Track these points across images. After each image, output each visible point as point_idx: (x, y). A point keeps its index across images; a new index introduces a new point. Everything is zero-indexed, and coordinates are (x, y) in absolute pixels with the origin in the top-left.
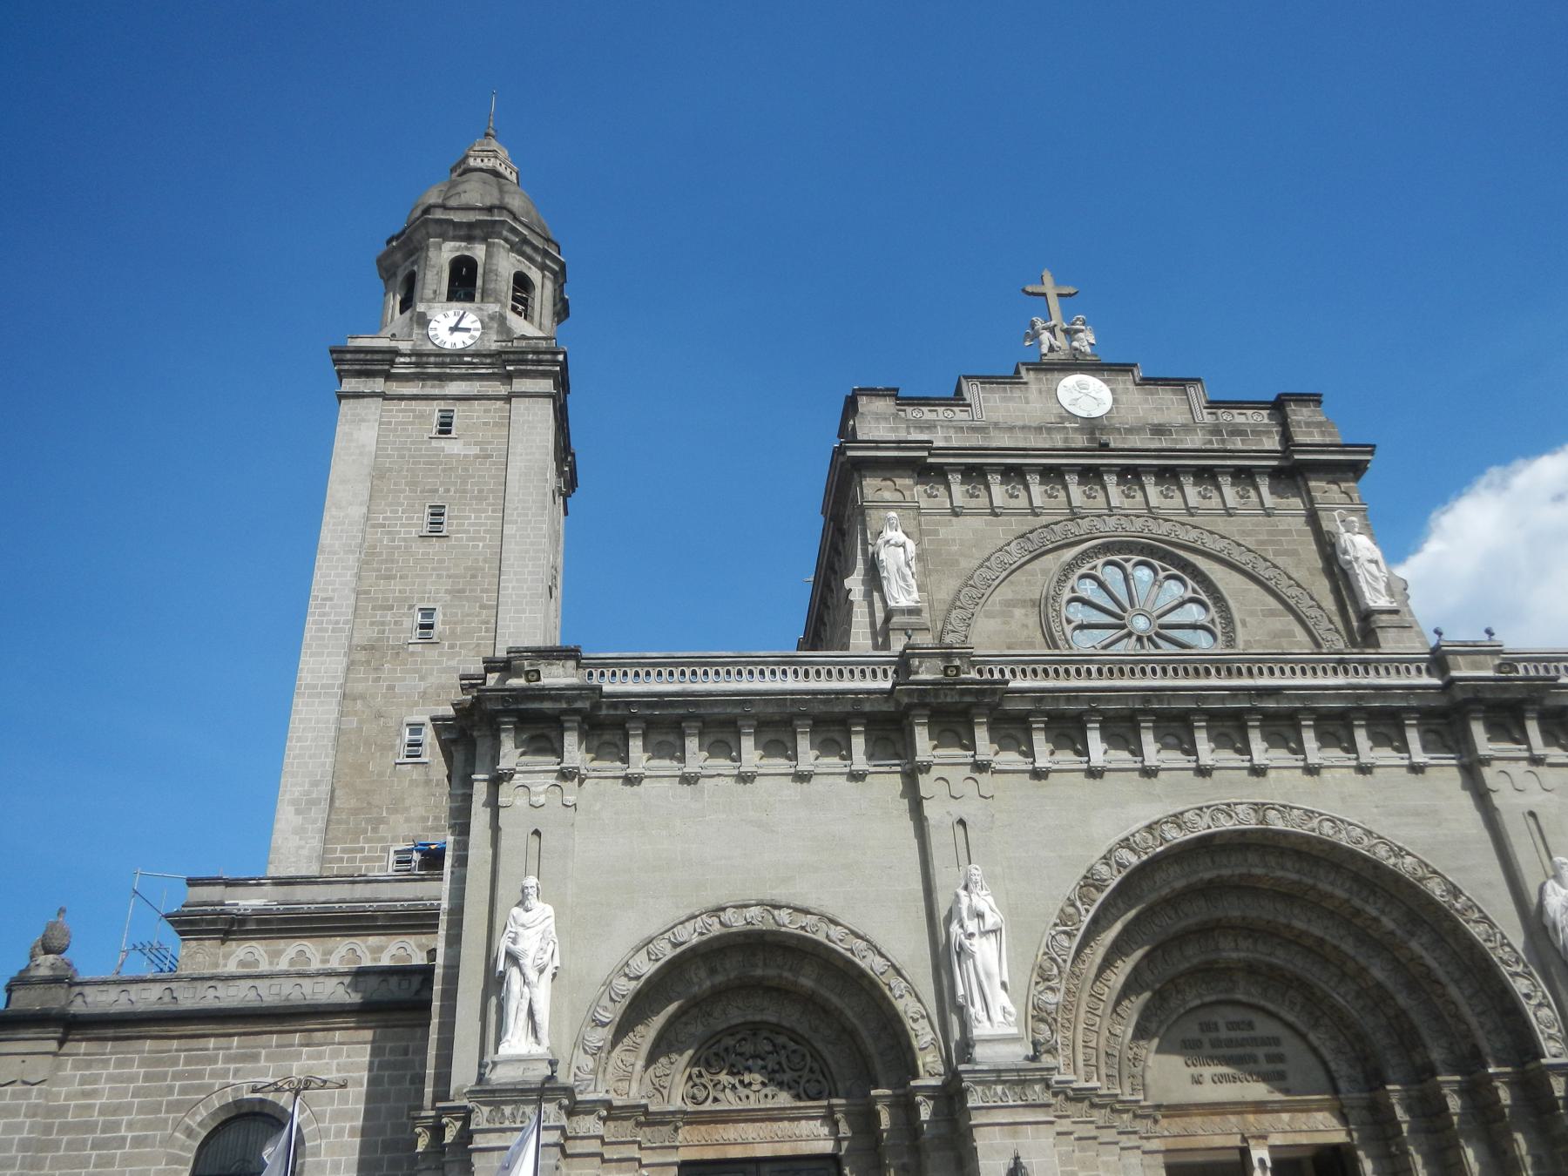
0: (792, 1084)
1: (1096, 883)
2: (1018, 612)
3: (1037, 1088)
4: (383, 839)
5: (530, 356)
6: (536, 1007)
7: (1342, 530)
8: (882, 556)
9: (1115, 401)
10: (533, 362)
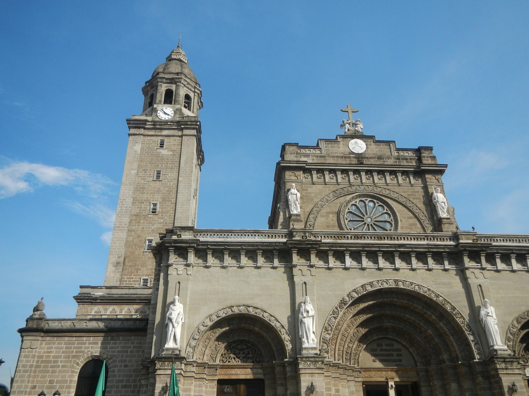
0: (252, 358)
1: (345, 302)
2: (331, 216)
3: (320, 363)
4: (139, 275)
5: (189, 123)
6: (176, 334)
7: (435, 192)
8: (290, 197)
9: (367, 148)
10: (190, 125)
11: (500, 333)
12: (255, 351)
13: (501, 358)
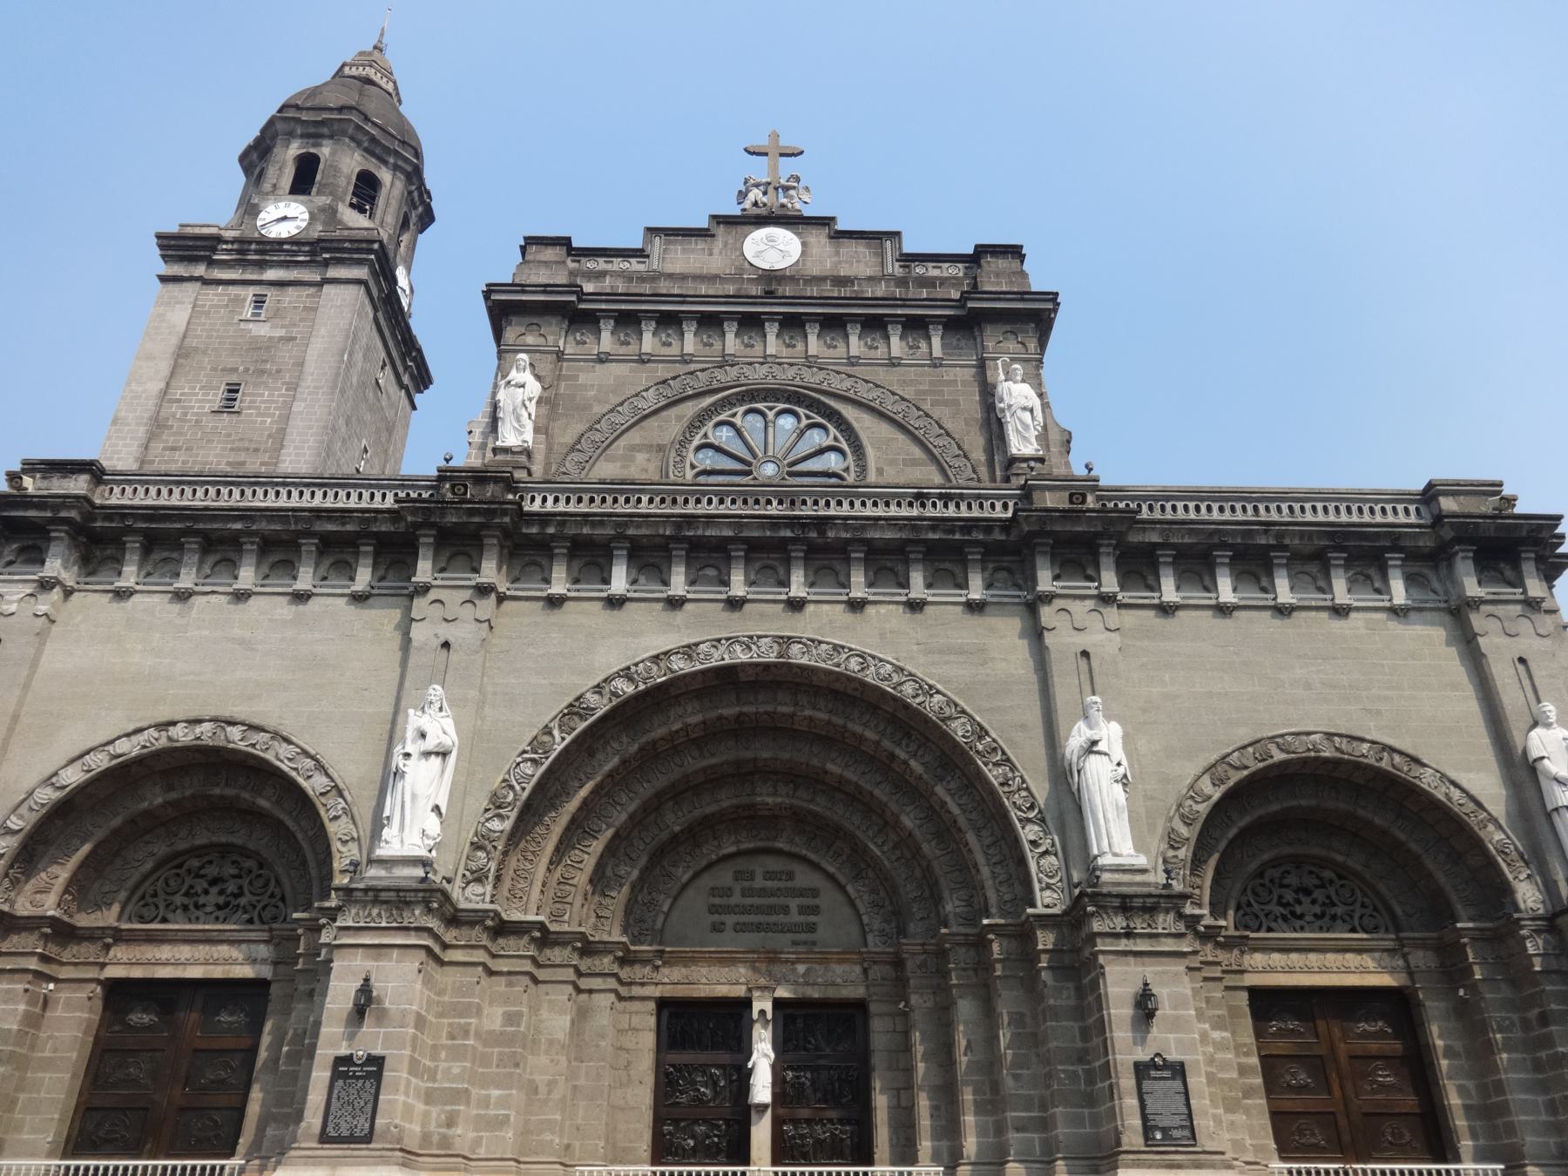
0: (250, 908)
2: (641, 457)
9: (803, 253)
11: (1129, 811)
12: (266, 885)
13: (1110, 895)
